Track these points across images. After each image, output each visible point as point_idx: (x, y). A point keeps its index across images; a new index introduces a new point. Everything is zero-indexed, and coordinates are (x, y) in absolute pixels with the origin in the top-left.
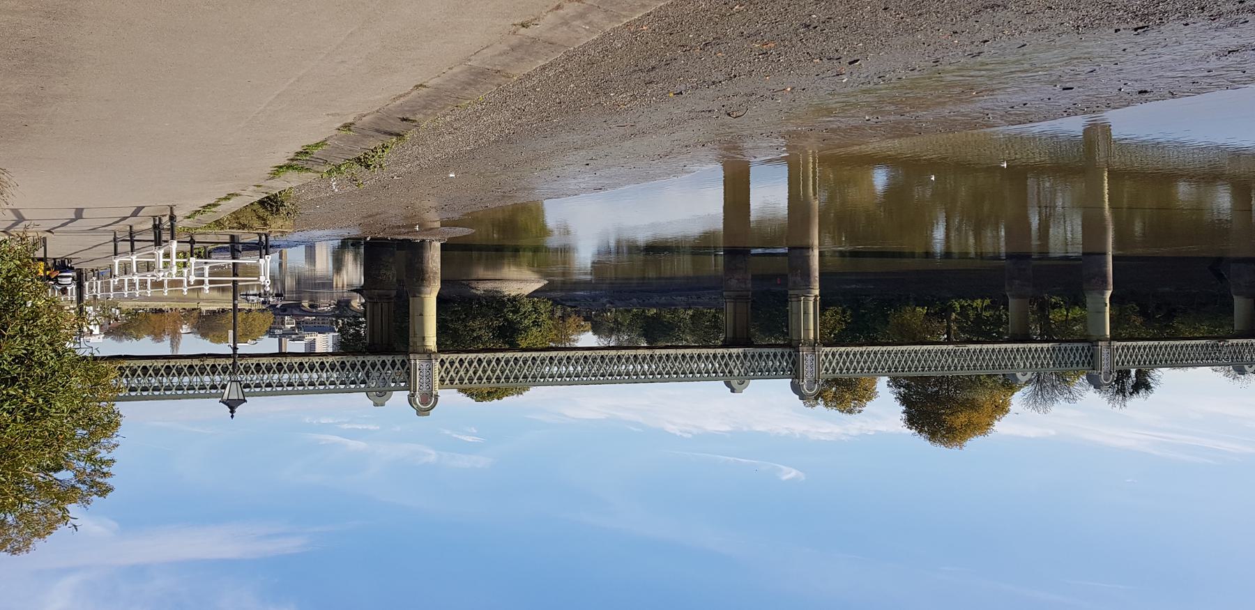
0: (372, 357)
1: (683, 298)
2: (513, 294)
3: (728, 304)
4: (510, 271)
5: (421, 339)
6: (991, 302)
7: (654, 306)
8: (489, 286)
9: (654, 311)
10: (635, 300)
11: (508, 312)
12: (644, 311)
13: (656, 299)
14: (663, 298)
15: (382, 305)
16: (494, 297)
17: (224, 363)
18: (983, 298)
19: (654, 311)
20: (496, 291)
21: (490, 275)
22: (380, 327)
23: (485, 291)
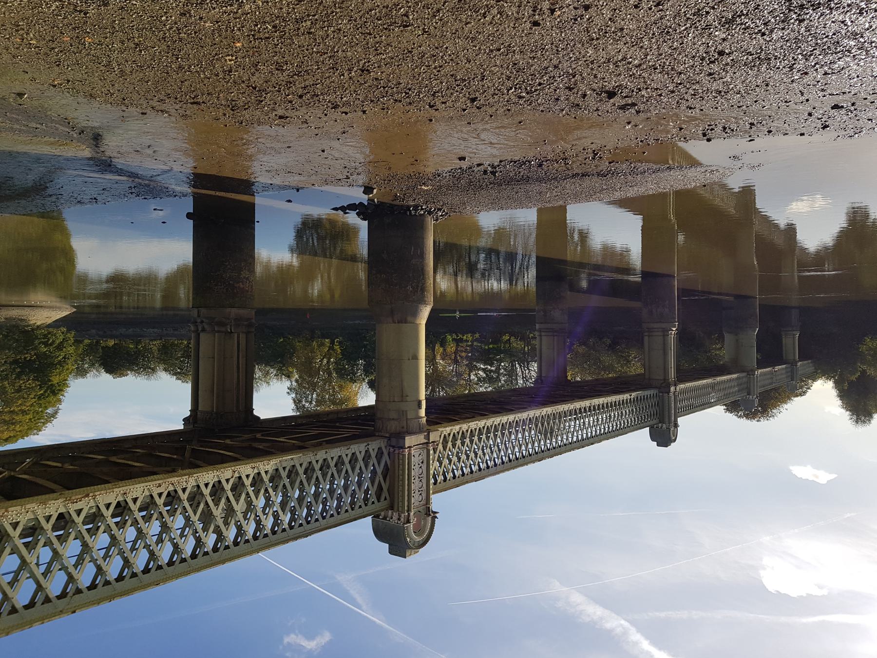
0: (335, 450)
1: (156, 330)
2: (39, 323)
3: (544, 338)
4: (38, 296)
5: (416, 403)
6: (480, 336)
7: (112, 337)
8: (14, 313)
9: (111, 343)
10: (94, 331)
11: (39, 344)
12: (98, 342)
13: (123, 331)
14: (131, 330)
15: (238, 337)
16: (16, 326)
17: (30, 516)
18: (473, 333)
19: (111, 343)
20: (22, 320)
21: (14, 299)
22: (235, 381)
23: (6, 319)
